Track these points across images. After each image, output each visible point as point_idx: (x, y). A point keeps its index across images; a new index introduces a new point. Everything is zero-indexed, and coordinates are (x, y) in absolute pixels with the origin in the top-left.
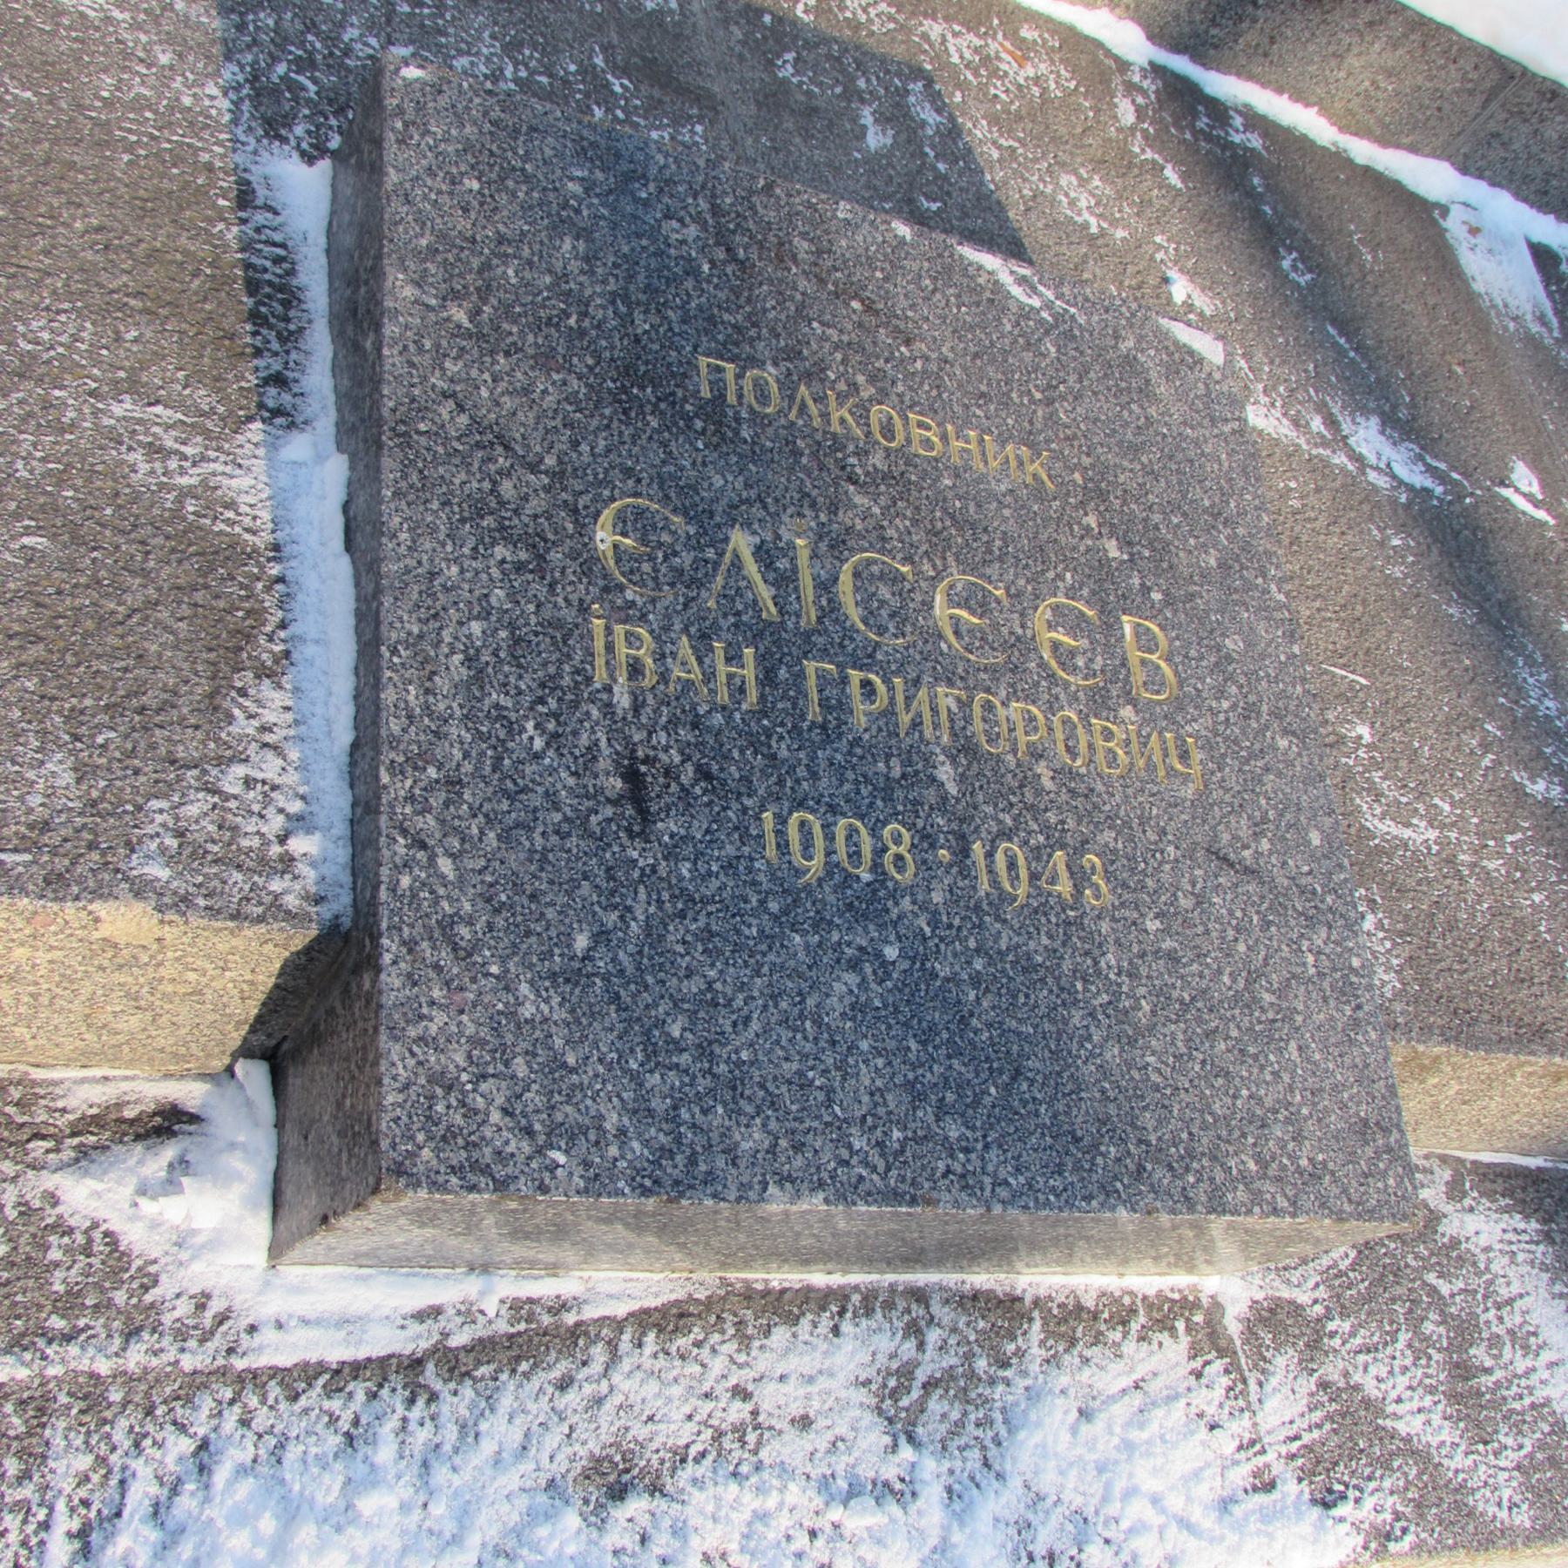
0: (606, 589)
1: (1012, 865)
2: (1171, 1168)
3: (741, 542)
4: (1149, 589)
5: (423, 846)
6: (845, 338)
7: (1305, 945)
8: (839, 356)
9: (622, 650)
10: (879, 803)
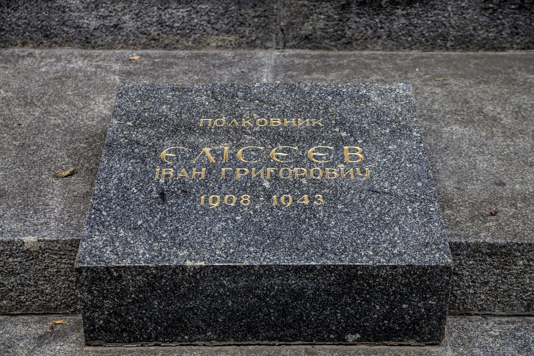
0: (162, 163)
1: (287, 199)
2: (335, 254)
3: (207, 150)
4: (357, 140)
5: (99, 210)
6: (251, 108)
7: (408, 207)
8: (248, 112)
9: (164, 173)
10: (241, 192)
